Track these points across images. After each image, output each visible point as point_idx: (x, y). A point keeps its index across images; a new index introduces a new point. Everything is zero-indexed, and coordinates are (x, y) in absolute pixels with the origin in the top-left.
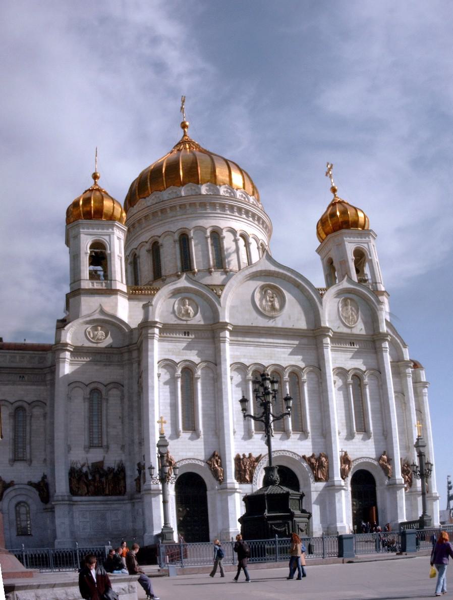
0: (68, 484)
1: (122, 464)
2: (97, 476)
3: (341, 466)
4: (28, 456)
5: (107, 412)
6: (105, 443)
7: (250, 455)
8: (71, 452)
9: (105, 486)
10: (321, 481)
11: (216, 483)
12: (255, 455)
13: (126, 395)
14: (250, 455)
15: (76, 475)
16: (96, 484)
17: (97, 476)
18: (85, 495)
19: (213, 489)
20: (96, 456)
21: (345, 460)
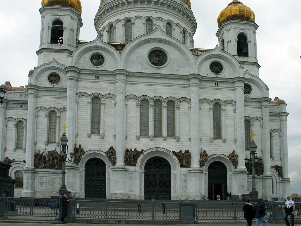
3: (200, 158)
7: (135, 149)
10: (185, 167)
11: (111, 165)
12: (139, 149)
14: (135, 149)
19: (109, 167)
21: (203, 155)
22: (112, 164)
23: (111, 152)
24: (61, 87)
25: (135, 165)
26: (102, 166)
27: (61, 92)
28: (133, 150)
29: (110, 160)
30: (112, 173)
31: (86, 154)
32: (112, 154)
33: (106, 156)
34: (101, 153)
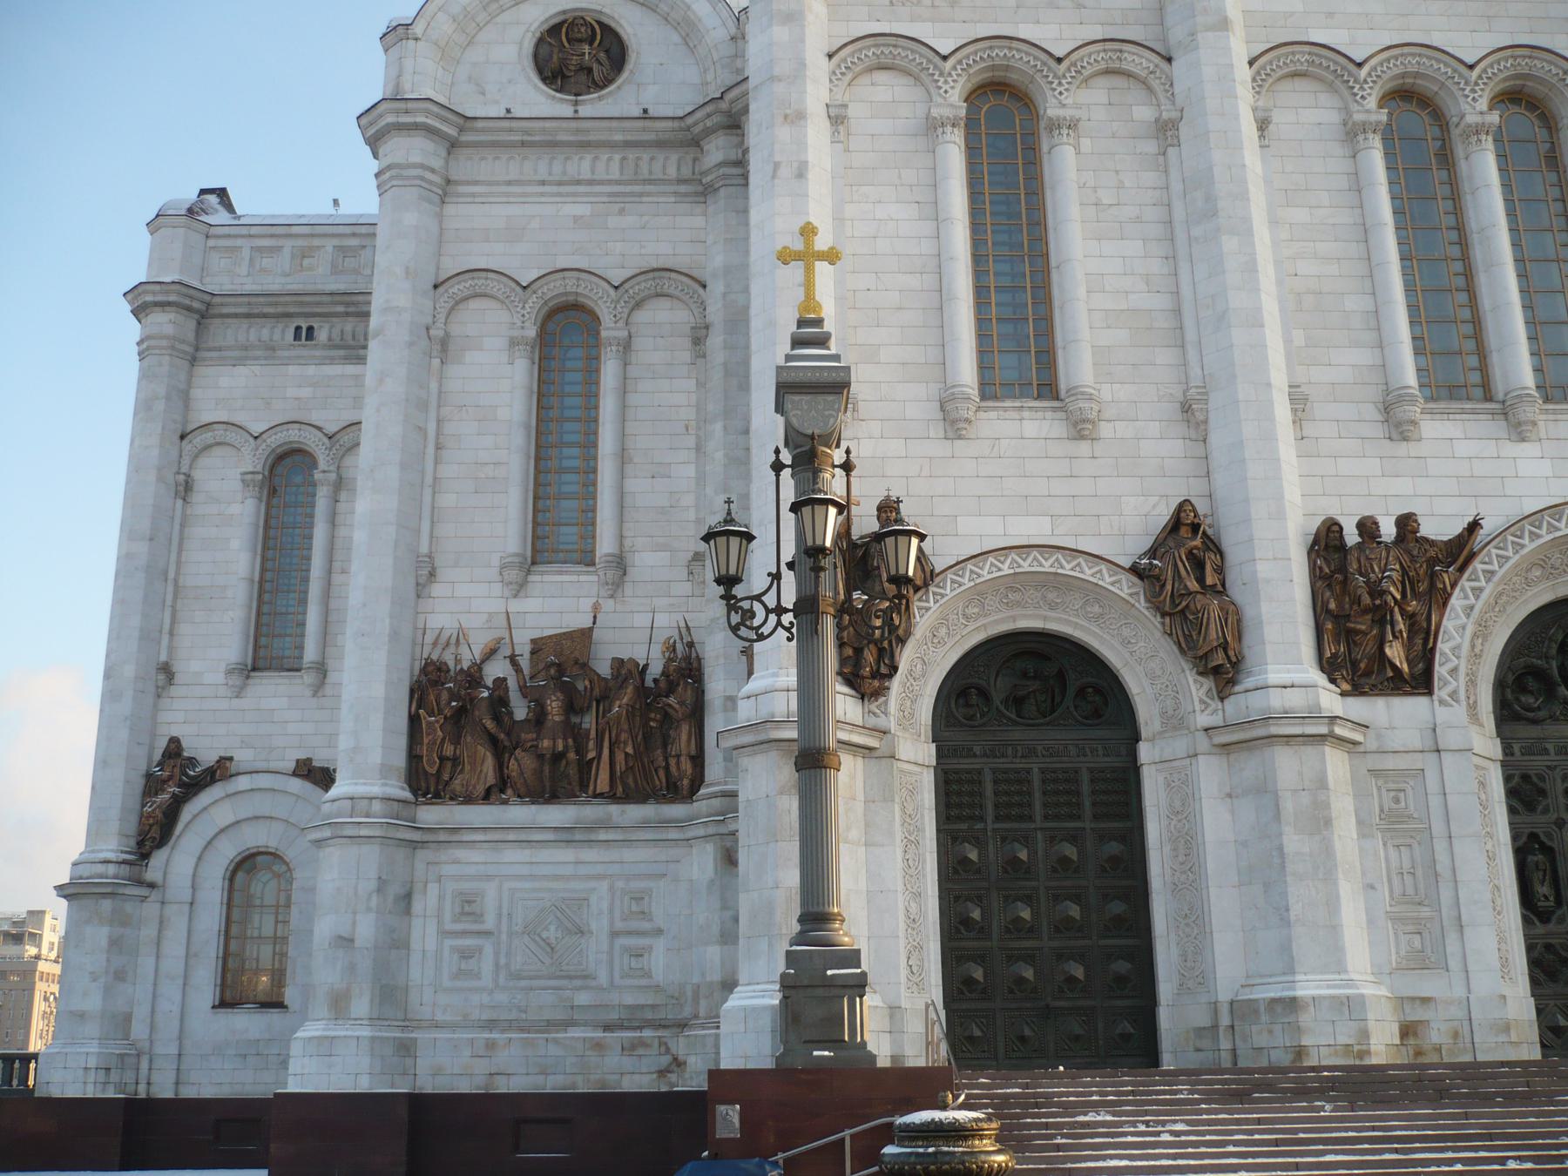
0: (402, 742)
1: (691, 645)
2: (554, 705)
4: (310, 653)
5: (623, 407)
6: (605, 545)
7: (1406, 523)
8: (437, 589)
9: (591, 755)
11: (1196, 688)
12: (1439, 527)
13: (715, 312)
14: (1406, 523)
15: (445, 696)
16: (546, 743)
17: (554, 705)
18: (487, 797)
19: (1175, 722)
20: (556, 604)
22: (1208, 683)
23: (1186, 568)
24: (637, 112)
25: (1421, 681)
26: (1097, 714)
27: (631, 155)
28: (1388, 530)
29: (1188, 637)
30: (1210, 774)
31: (948, 590)
32: (1201, 580)
33: (1141, 604)
34: (1088, 572)
